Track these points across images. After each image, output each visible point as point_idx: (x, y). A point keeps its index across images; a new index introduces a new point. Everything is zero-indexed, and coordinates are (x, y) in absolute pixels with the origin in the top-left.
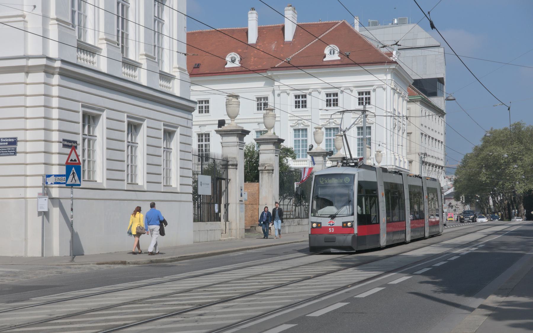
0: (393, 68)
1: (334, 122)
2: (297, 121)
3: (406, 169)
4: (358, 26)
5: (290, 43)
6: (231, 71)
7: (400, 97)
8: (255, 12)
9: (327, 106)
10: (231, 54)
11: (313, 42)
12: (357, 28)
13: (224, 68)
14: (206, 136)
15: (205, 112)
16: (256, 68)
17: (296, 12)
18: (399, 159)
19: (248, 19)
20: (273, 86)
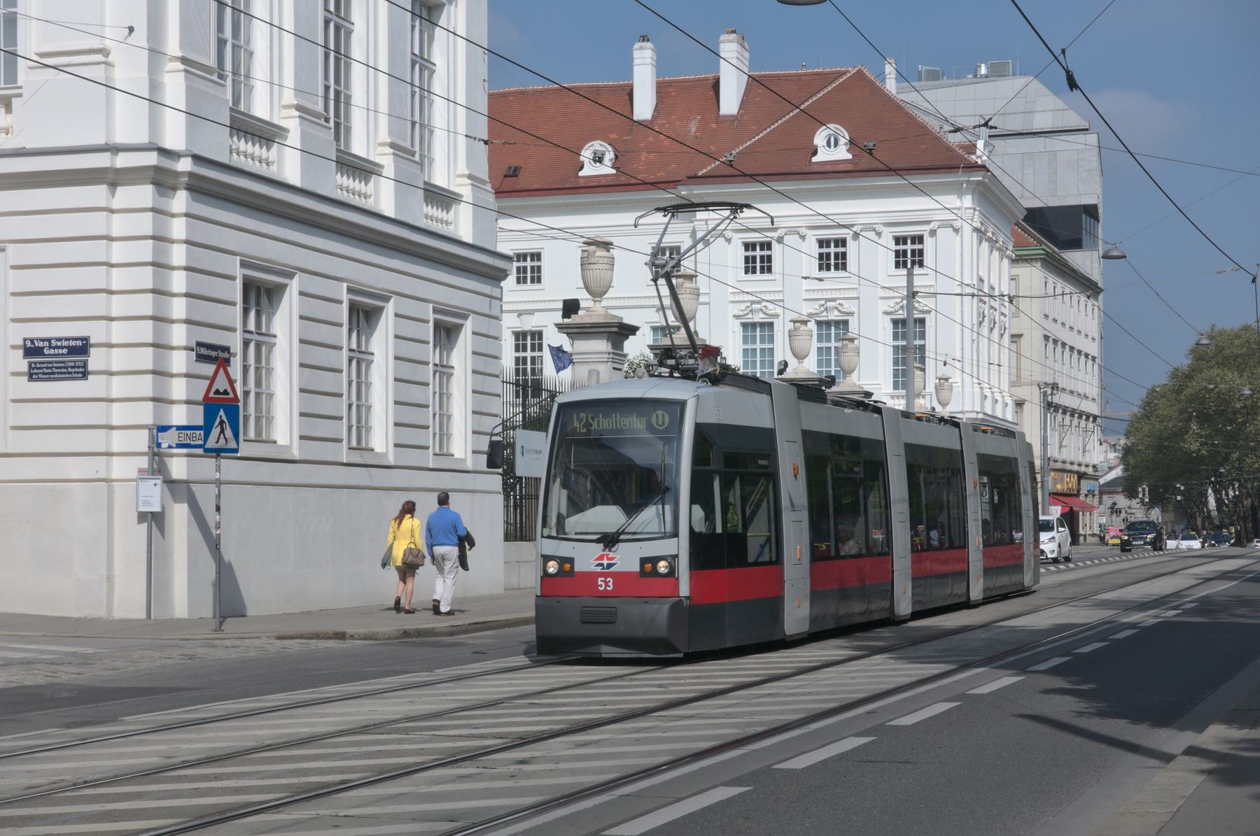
0: (978, 181)
1: (836, 308)
2: (749, 304)
3: (1009, 422)
4: (893, 81)
5: (731, 119)
6: (592, 184)
7: (994, 250)
9: (819, 271)
10: (592, 145)
11: (788, 117)
12: (891, 85)
13: (577, 176)
14: (533, 339)
15: (533, 282)
16: (652, 178)
18: (993, 397)
20: (693, 222)
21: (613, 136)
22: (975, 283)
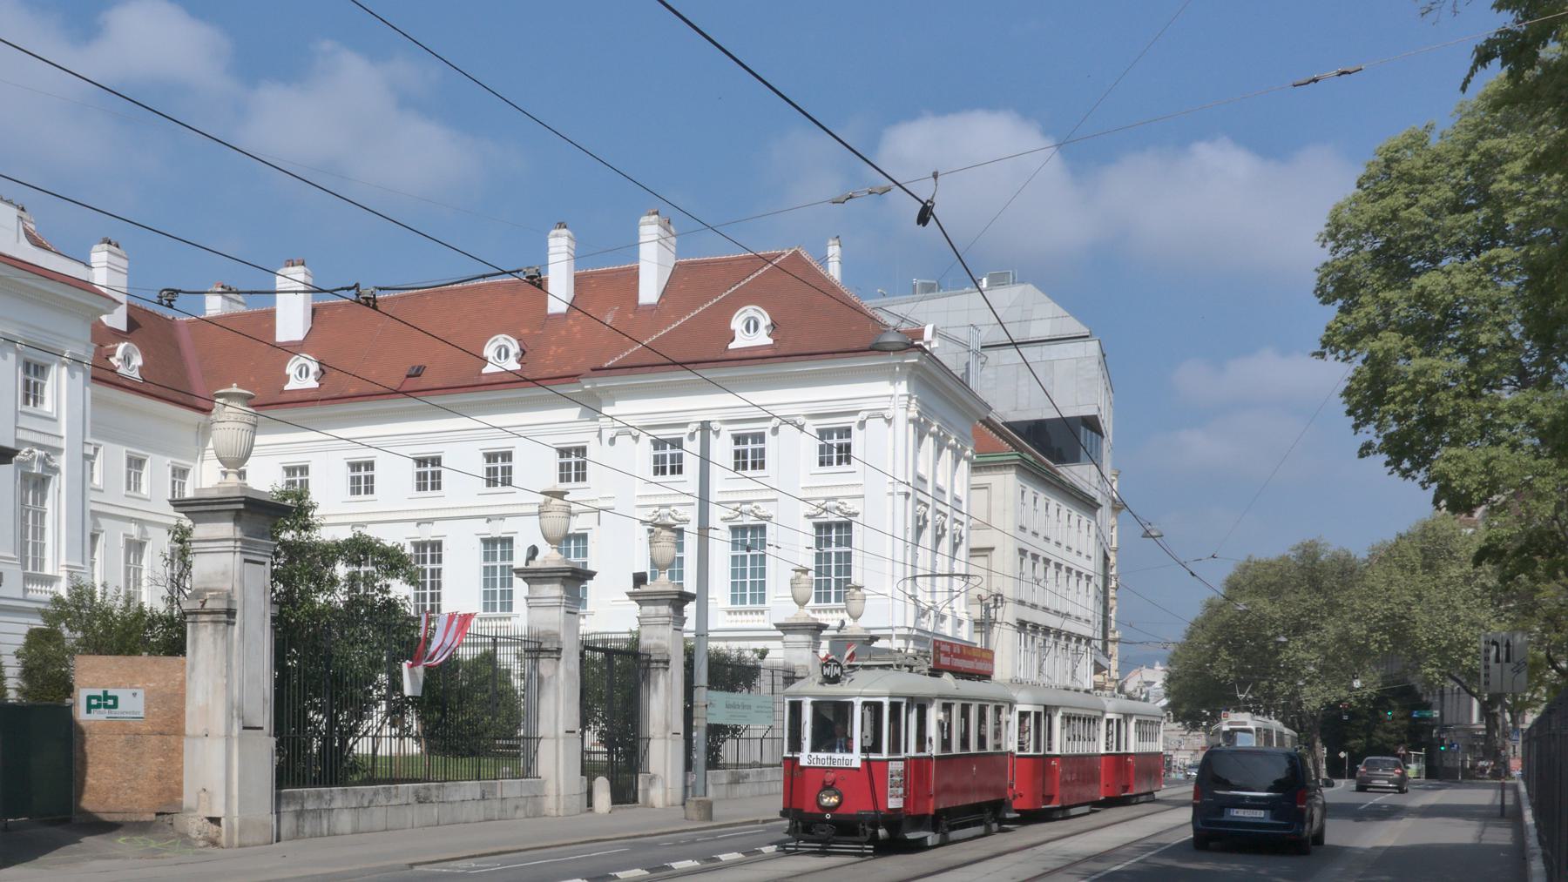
8: (565, 231)
13: (480, 374)
14: (433, 550)
17: (673, 230)
19: (548, 250)
20: (597, 420)
21: (525, 331)
22: (910, 481)
